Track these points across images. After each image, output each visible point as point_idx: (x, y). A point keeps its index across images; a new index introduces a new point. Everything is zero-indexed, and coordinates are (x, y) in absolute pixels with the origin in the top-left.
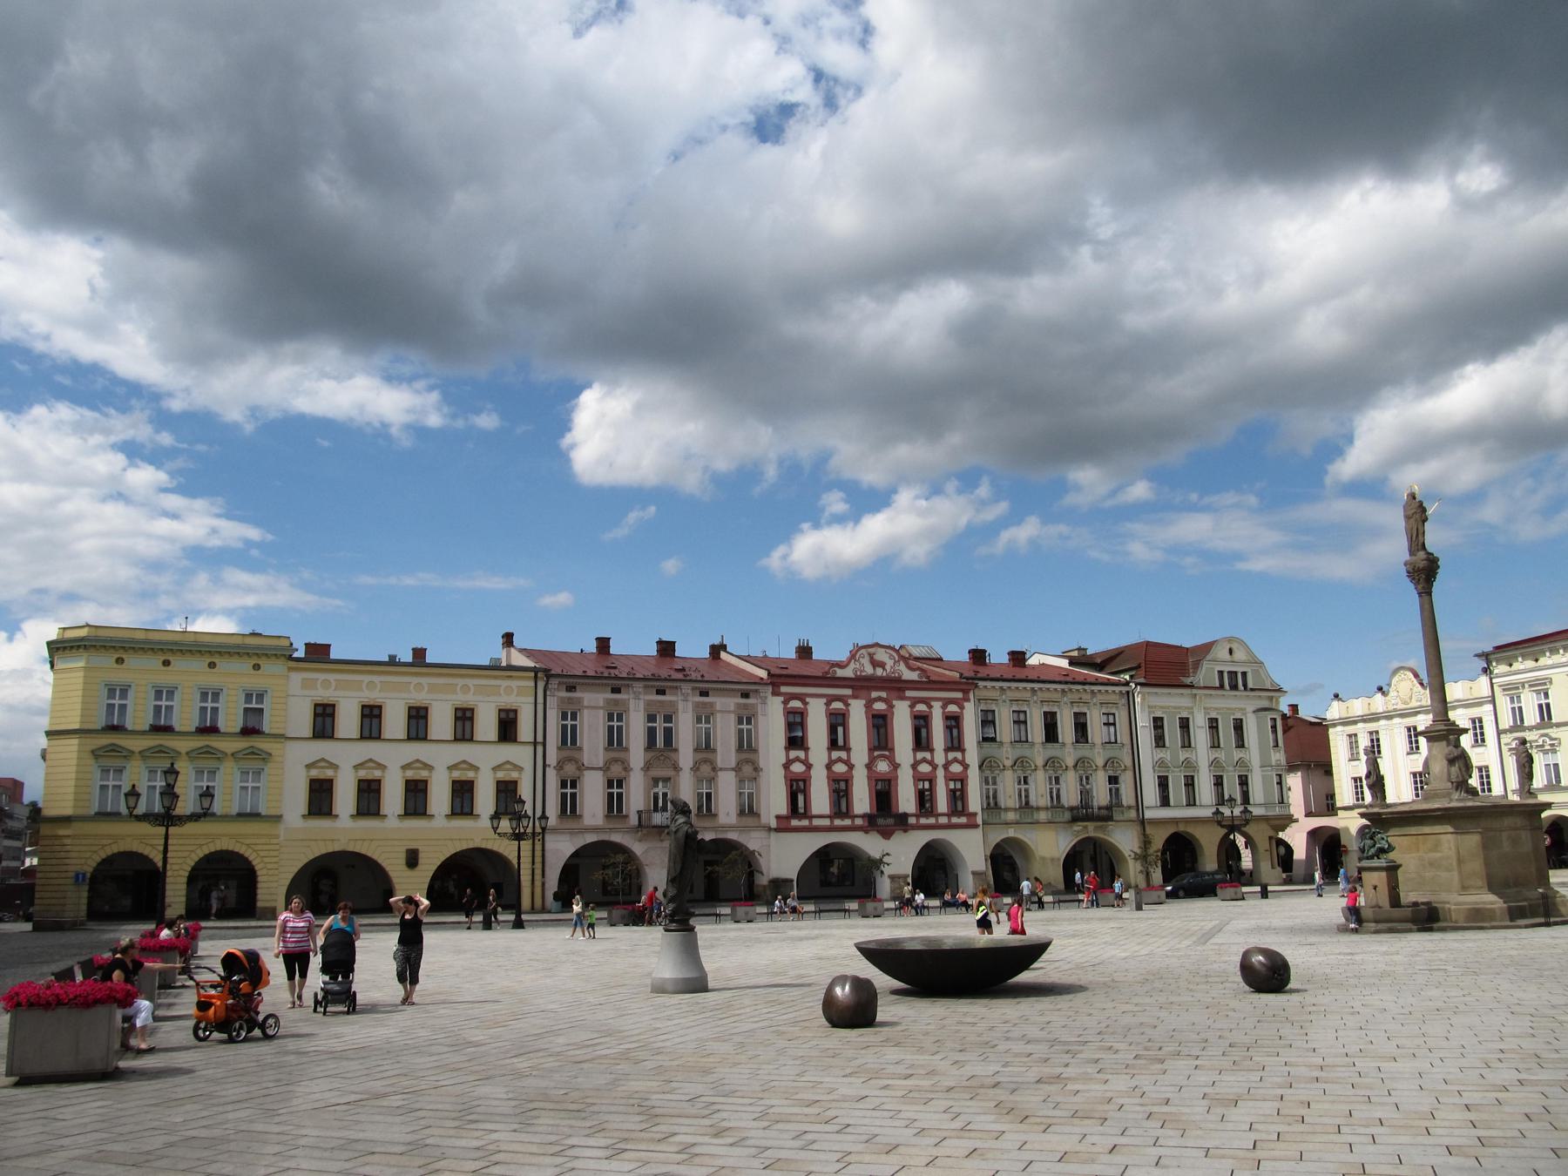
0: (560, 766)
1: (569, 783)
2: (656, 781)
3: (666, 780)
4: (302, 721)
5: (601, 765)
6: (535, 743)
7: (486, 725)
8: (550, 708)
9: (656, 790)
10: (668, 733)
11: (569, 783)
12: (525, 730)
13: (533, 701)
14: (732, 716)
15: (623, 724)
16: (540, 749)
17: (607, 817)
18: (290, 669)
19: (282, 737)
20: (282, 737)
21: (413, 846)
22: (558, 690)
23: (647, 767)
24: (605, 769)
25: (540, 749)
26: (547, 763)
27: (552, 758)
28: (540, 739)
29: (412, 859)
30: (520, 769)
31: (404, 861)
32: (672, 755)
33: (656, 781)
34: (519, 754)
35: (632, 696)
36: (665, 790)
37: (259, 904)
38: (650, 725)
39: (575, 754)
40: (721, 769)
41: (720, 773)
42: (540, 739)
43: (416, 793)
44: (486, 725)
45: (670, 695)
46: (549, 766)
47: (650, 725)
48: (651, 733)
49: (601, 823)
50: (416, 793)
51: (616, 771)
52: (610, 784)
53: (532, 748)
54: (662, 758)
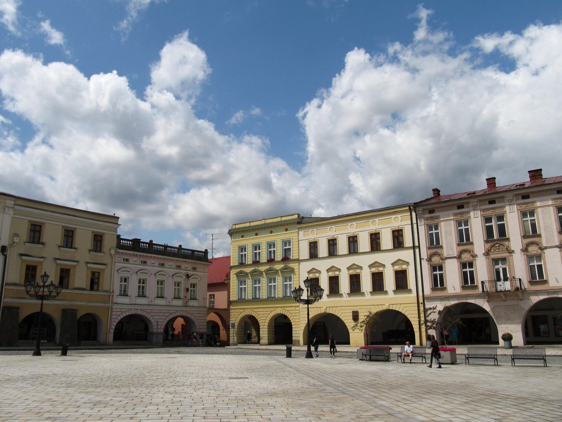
0: (429, 260)
1: (437, 268)
2: (496, 261)
3: (504, 260)
4: (305, 253)
5: (456, 255)
6: (414, 247)
7: (387, 241)
8: (420, 225)
9: (497, 267)
10: (502, 230)
11: (437, 268)
12: (408, 241)
13: (410, 223)
14: (551, 208)
15: (469, 227)
16: (417, 250)
17: (463, 288)
18: (299, 229)
19: (298, 261)
20: (298, 261)
21: (355, 309)
22: (424, 214)
23: (487, 254)
24: (459, 257)
25: (417, 250)
26: (422, 258)
27: (424, 255)
28: (417, 244)
29: (355, 316)
30: (408, 263)
31: (351, 318)
32: (506, 243)
33: (496, 261)
34: (406, 255)
35: (471, 209)
36: (504, 266)
37: (293, 338)
38: (487, 224)
39: (439, 251)
40: (546, 248)
41: (545, 251)
42: (417, 244)
43: (355, 281)
44: (387, 241)
45: (499, 202)
46: (423, 259)
47: (487, 224)
48: (489, 231)
49: (459, 291)
50: (355, 281)
51: (466, 257)
52: (464, 265)
53: (412, 251)
54: (497, 245)
